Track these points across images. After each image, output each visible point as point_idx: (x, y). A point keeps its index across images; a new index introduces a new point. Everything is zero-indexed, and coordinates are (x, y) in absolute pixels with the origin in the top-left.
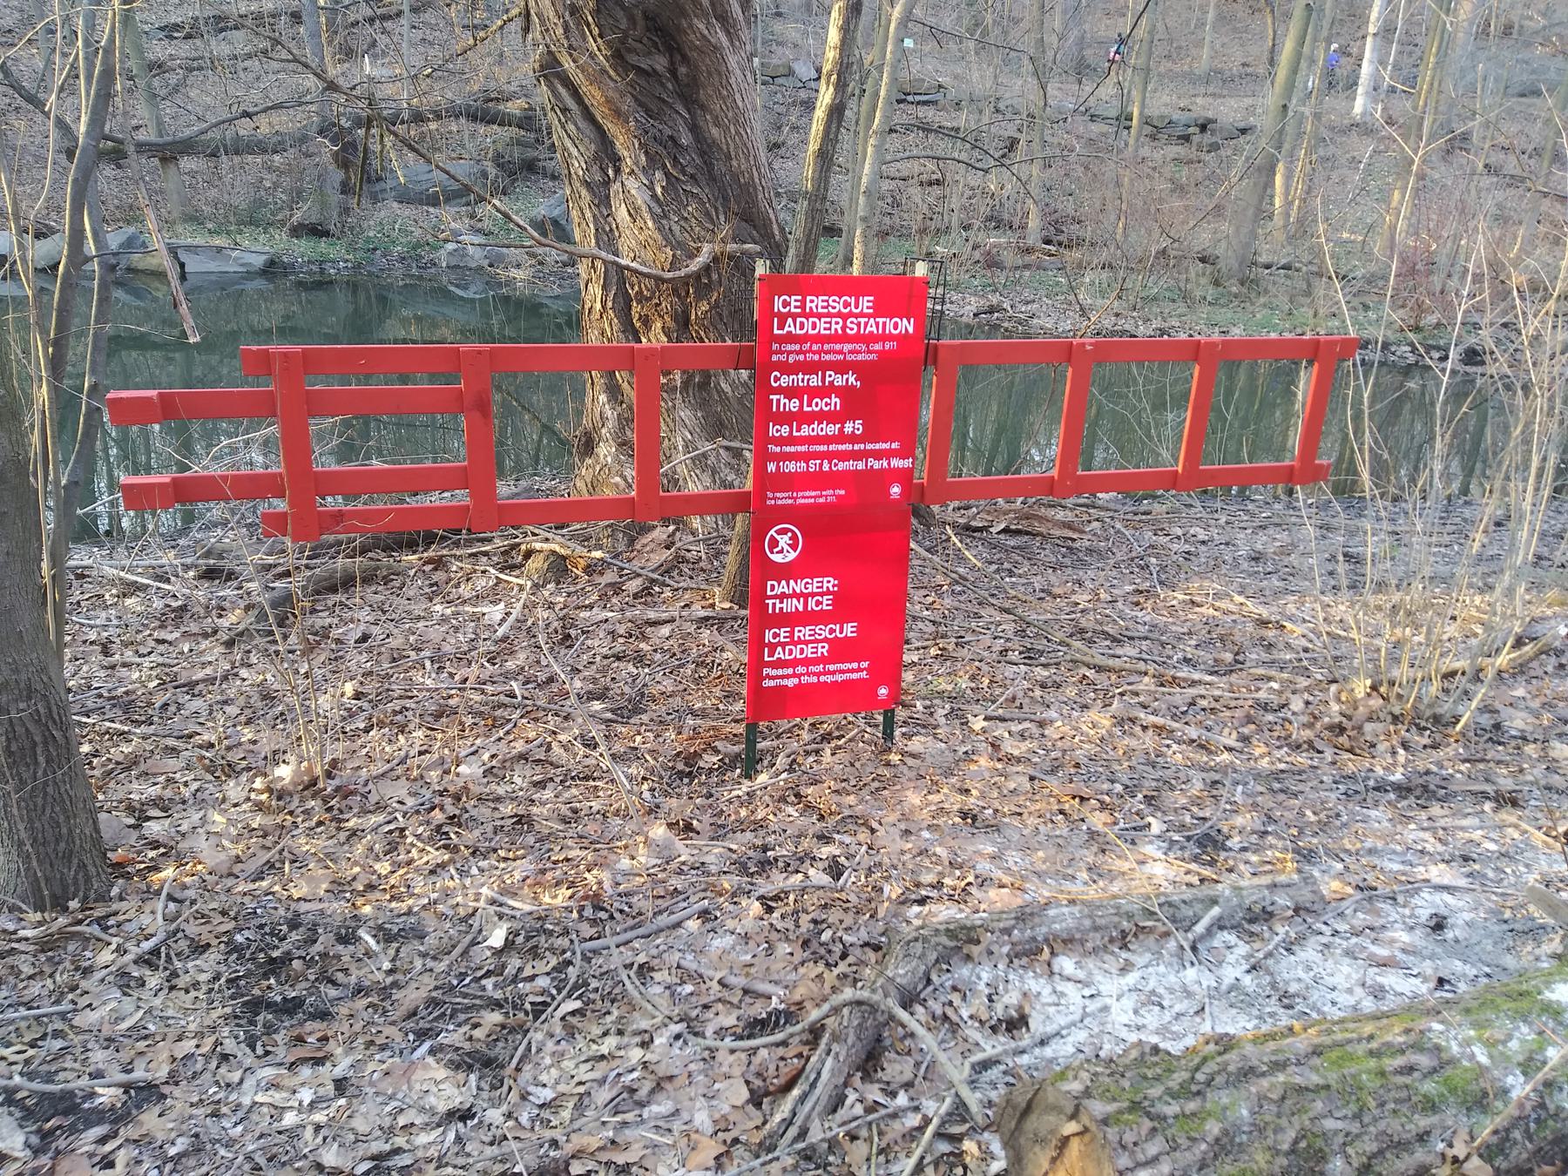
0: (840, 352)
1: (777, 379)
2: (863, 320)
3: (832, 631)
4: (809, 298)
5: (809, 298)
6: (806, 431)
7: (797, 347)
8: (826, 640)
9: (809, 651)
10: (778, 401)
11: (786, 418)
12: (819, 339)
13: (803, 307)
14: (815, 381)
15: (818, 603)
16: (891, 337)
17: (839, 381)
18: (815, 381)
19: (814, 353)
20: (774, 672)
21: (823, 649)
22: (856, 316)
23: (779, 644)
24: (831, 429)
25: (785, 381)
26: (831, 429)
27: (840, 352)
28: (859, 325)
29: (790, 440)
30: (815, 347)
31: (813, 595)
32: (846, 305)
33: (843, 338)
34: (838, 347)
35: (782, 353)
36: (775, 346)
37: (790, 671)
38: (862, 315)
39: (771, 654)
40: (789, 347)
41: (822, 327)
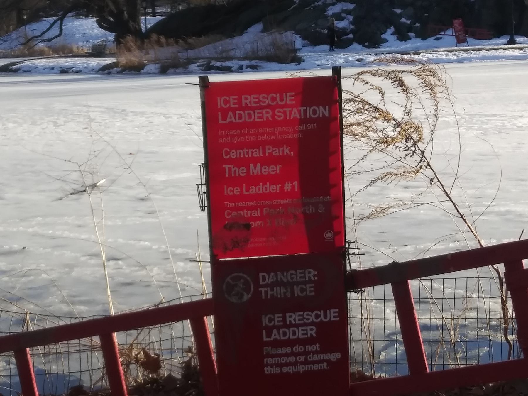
0: (273, 134)
1: (227, 153)
2: (288, 110)
3: (317, 316)
4: (243, 97)
5: (243, 97)
6: (253, 190)
7: (238, 132)
8: (313, 323)
9: (300, 333)
10: (230, 169)
11: (235, 181)
12: (254, 125)
13: (240, 102)
14: (257, 153)
15: (303, 290)
16: (311, 120)
17: (277, 152)
18: (257, 153)
19: (252, 135)
20: (273, 352)
21: (312, 331)
22: (283, 107)
23: (274, 327)
24: (274, 188)
25: (234, 154)
26: (274, 188)
27: (273, 134)
28: (285, 113)
29: (242, 198)
30: (252, 131)
31: (298, 283)
32: (273, 99)
33: (274, 123)
34: (269, 130)
35: (226, 136)
36: (221, 132)
37: (288, 350)
38: (286, 106)
39: (269, 335)
40: (232, 132)
41: (256, 116)
